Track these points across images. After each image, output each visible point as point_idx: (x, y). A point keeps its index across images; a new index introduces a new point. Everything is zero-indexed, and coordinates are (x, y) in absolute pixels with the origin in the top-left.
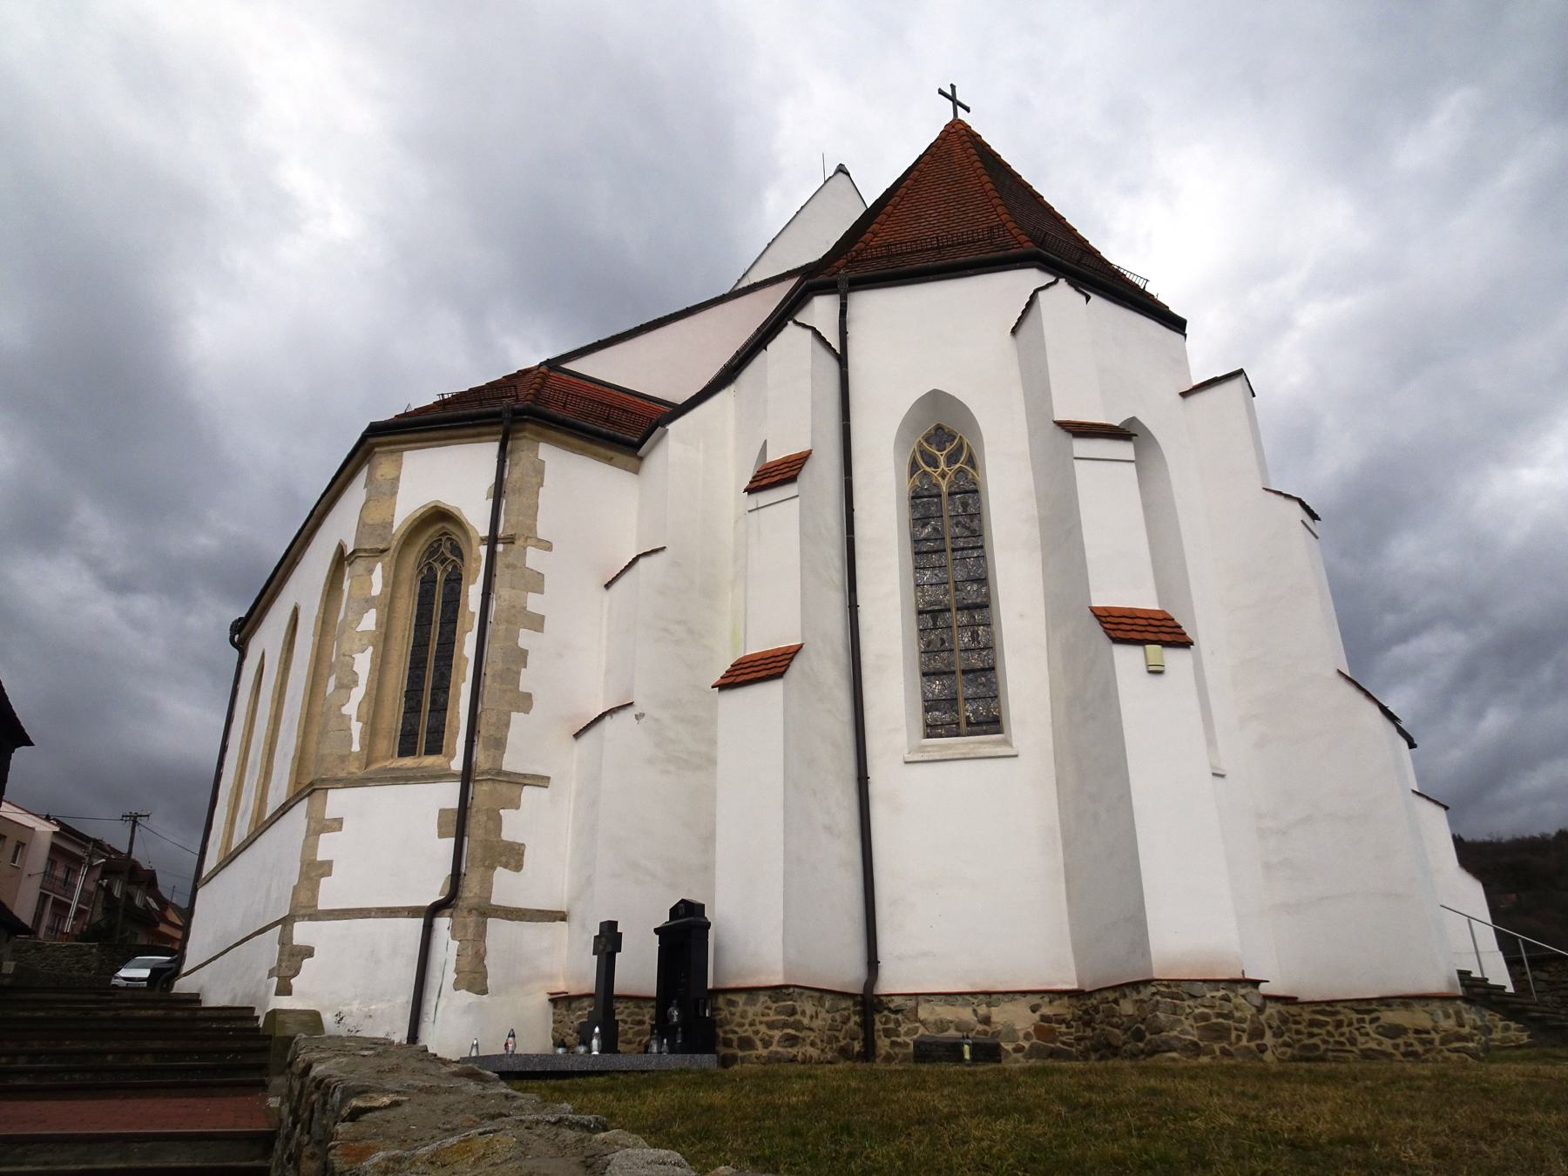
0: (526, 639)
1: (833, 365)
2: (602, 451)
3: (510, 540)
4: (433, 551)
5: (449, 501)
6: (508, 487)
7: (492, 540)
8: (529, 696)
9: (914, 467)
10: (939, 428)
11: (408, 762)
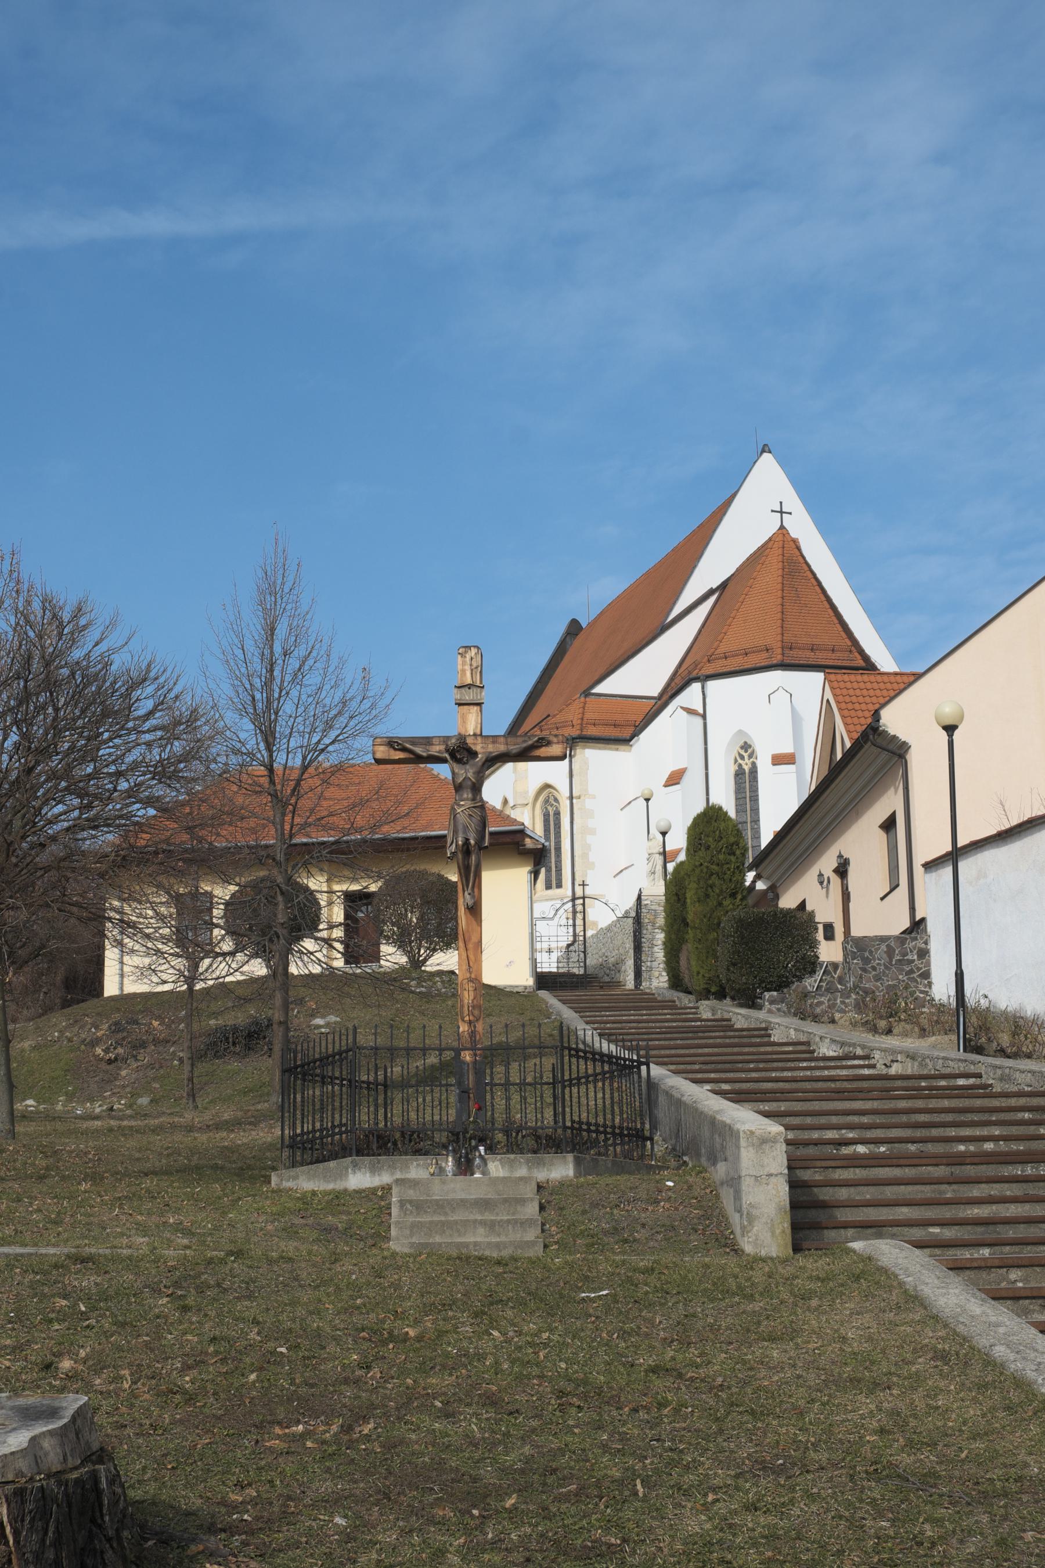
0: (589, 839)
1: (699, 721)
2: (613, 746)
3: (579, 797)
4: (547, 801)
5: (550, 782)
6: (574, 772)
7: (571, 798)
8: (593, 863)
9: (736, 761)
10: (745, 743)
11: (549, 892)
